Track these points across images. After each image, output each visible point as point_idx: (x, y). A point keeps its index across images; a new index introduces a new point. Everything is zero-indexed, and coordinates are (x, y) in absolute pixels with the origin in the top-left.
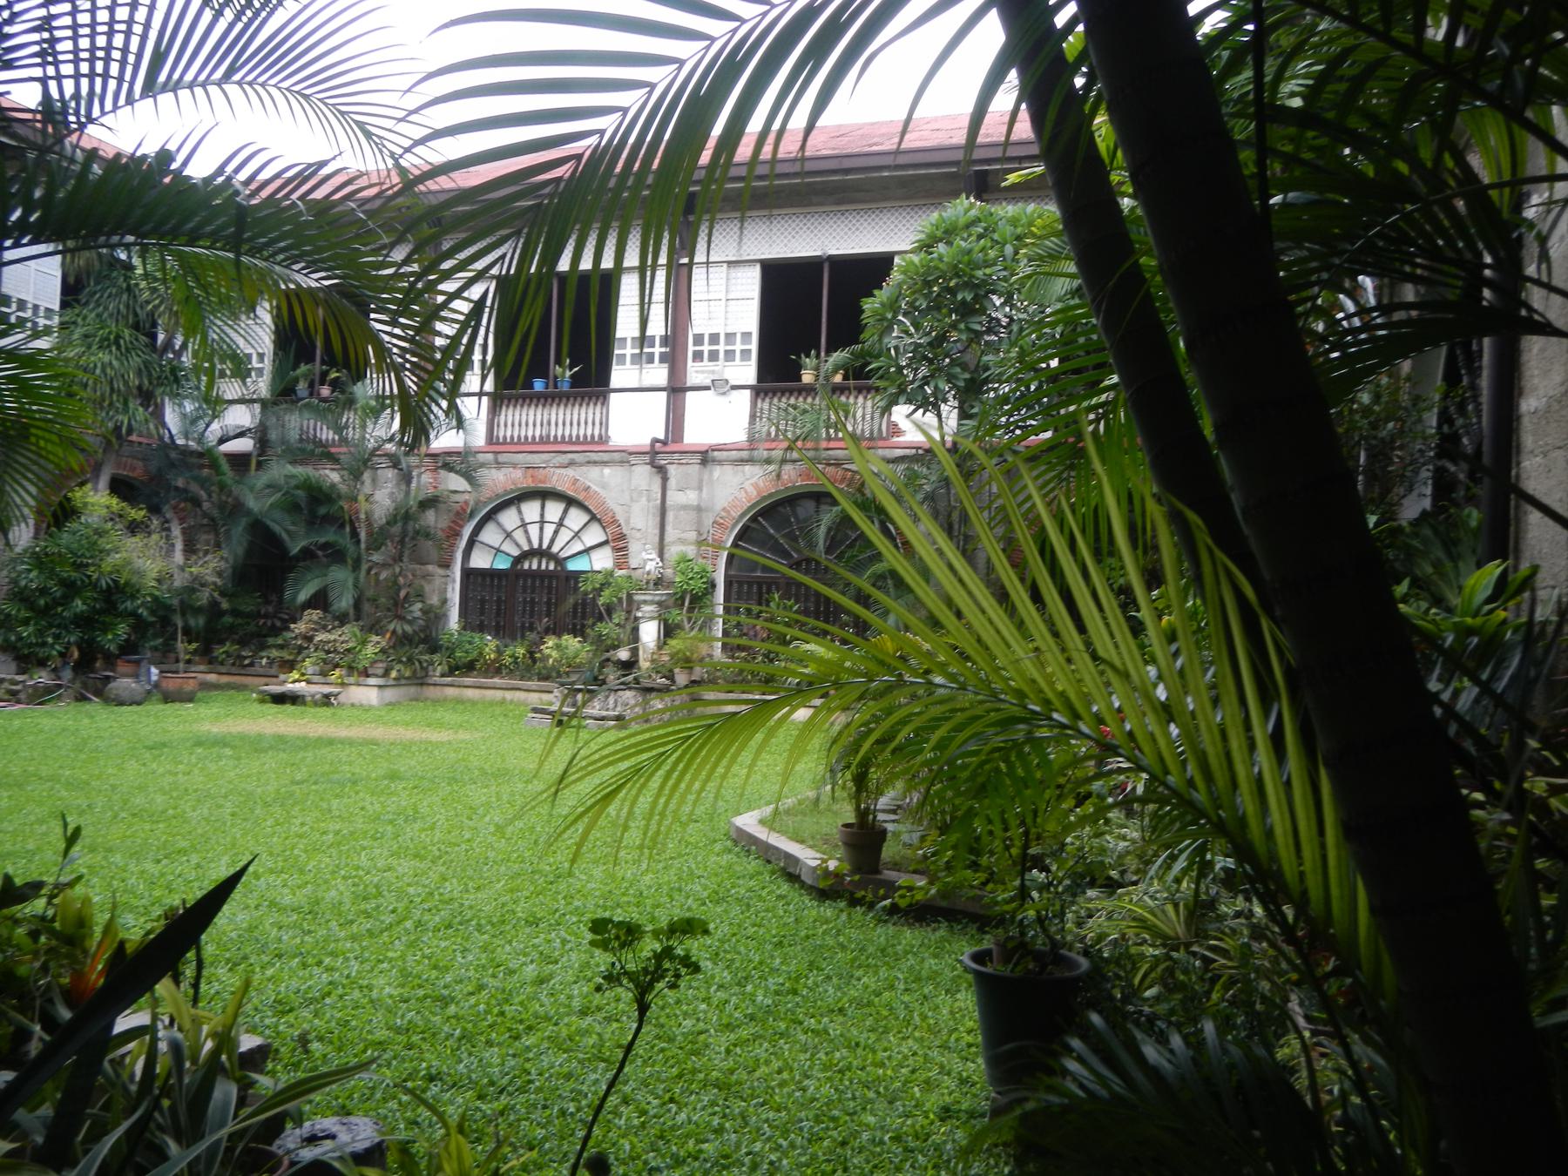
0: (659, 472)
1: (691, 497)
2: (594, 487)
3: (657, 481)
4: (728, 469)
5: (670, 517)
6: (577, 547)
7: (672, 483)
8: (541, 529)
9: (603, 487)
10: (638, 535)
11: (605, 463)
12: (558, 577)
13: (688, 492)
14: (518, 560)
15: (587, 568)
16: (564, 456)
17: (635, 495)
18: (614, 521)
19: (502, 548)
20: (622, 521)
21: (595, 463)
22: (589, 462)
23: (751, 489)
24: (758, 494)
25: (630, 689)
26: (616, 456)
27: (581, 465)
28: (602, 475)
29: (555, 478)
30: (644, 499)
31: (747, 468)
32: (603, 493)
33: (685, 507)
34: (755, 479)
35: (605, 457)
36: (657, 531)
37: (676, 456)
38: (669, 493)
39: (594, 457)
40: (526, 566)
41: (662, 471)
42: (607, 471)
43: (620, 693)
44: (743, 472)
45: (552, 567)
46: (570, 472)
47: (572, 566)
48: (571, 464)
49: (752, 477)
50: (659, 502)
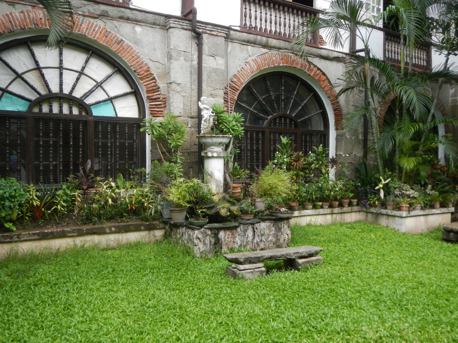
0: (194, 38)
1: (219, 63)
2: (126, 42)
3: (195, 46)
4: (237, 46)
5: (204, 77)
6: (99, 95)
7: (206, 48)
8: (61, 74)
9: (135, 43)
10: (178, 89)
11: (137, 22)
12: (86, 123)
13: (217, 58)
14: (33, 104)
15: (112, 114)
16: (96, 6)
17: (174, 54)
18: (149, 75)
19: (11, 89)
20: (155, 75)
21: (128, 19)
22: (121, 18)
23: (252, 63)
24: (259, 67)
25: (264, 220)
26: (151, 18)
27: (113, 18)
28: (135, 32)
29: (84, 26)
30: (182, 58)
31: (249, 48)
32: (135, 48)
33: (215, 70)
34: (254, 58)
35: (140, 16)
36: (195, 87)
37: (209, 27)
38: (204, 57)
39: (128, 13)
40: (45, 109)
41: (198, 37)
42: (138, 29)
43: (257, 225)
44: (247, 50)
45: (76, 111)
46: (99, 23)
47: (97, 112)
48: (103, 15)
49: (253, 55)
50: (195, 62)
